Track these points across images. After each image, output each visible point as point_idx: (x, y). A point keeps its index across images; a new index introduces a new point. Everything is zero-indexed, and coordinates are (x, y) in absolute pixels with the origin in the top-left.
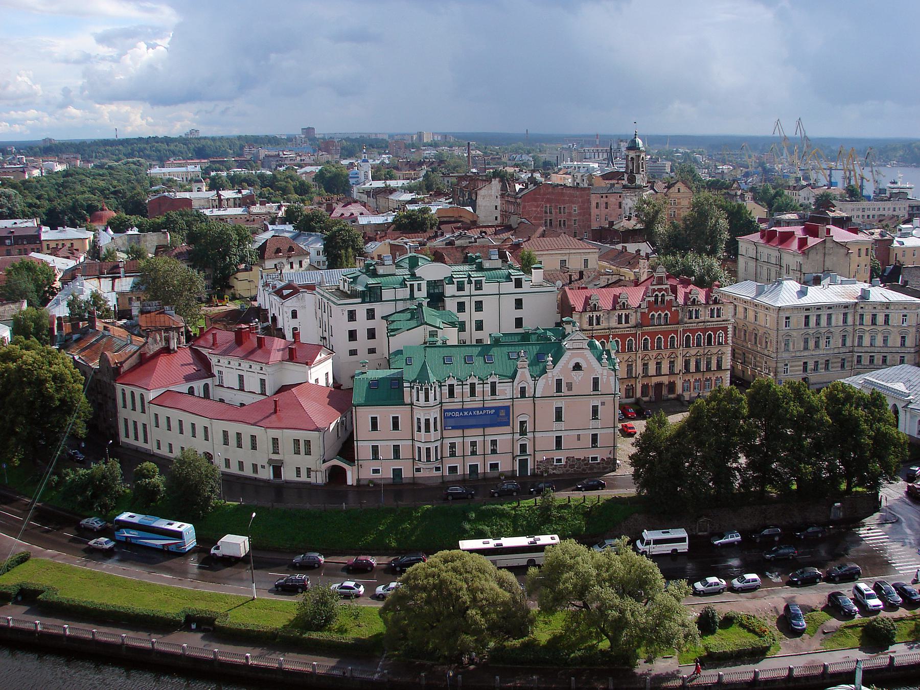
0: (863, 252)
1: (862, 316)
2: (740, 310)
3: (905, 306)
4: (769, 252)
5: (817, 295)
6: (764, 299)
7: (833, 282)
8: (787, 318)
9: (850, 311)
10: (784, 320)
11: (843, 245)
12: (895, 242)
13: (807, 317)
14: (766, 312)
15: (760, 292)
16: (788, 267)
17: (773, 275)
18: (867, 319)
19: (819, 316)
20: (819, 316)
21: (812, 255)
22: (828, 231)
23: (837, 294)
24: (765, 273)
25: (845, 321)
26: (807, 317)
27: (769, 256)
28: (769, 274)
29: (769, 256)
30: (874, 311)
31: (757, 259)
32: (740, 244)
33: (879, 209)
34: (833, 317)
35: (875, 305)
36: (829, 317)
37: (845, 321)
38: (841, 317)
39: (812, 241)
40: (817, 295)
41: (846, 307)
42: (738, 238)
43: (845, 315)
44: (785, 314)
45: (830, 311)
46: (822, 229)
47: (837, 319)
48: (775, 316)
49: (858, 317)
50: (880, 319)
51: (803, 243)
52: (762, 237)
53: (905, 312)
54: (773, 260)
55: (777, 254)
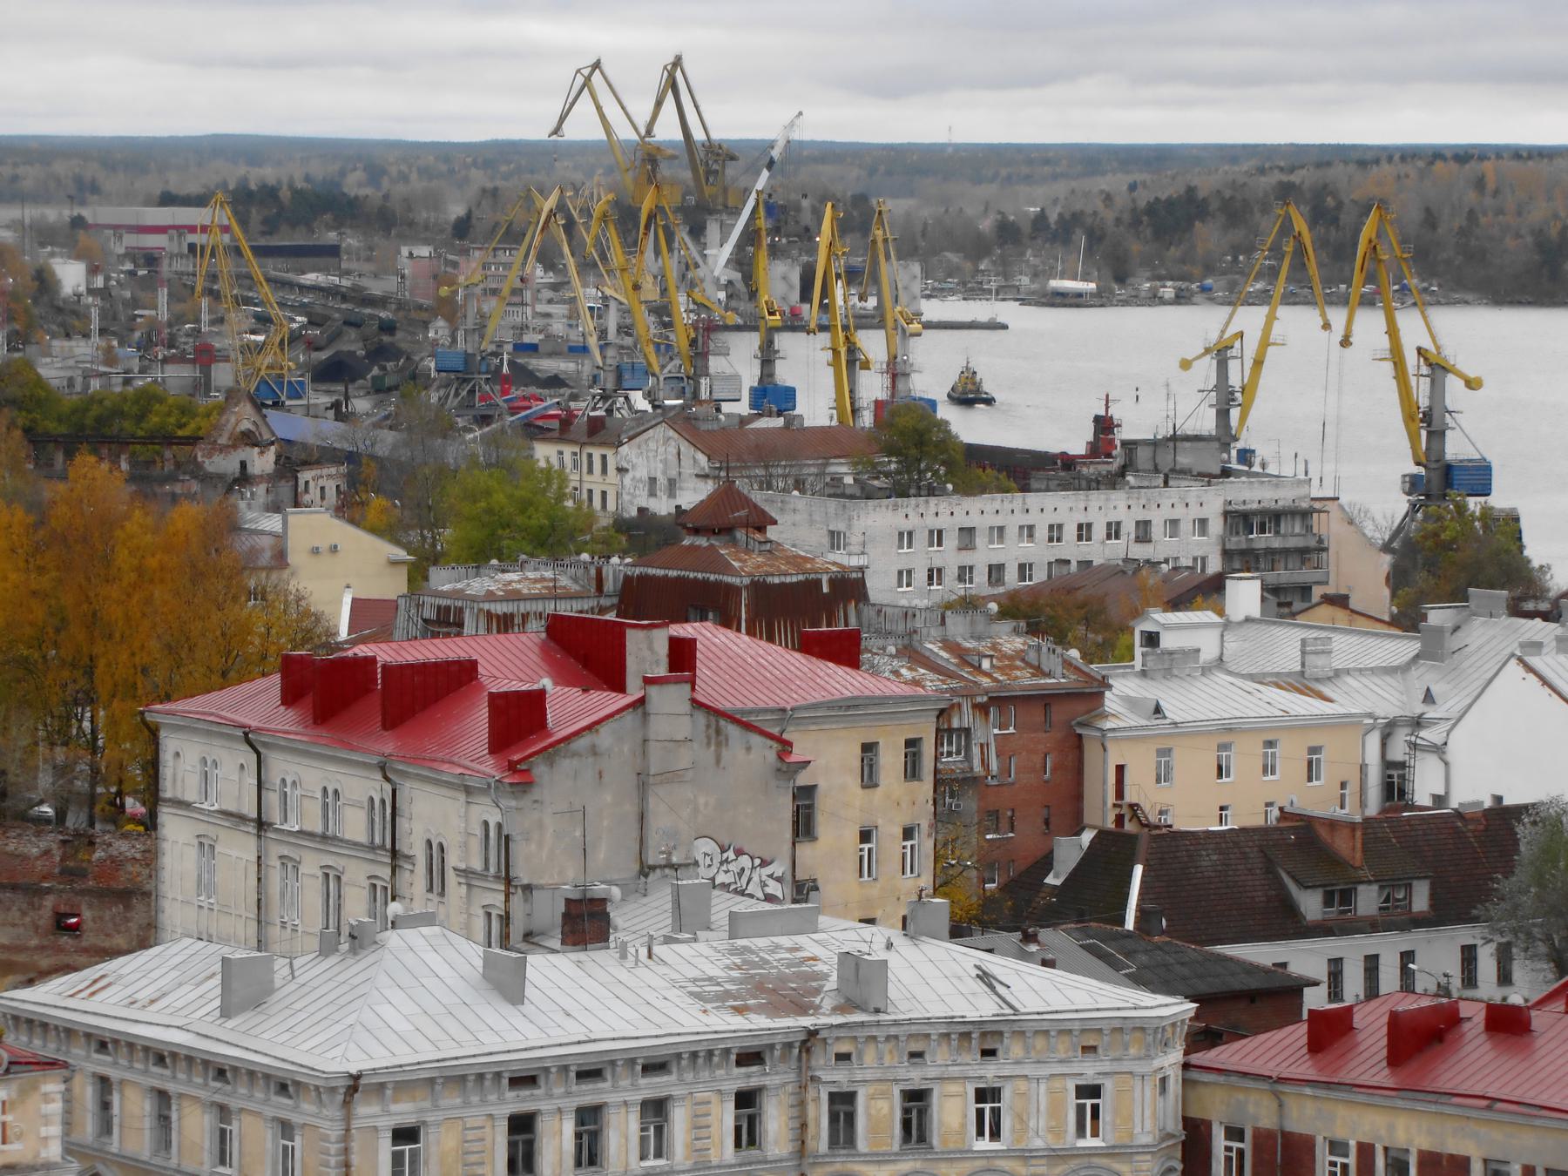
0: (891, 760)
1: (843, 1103)
2: (134, 1107)
3: (1088, 1037)
4: (329, 784)
5: (582, 1003)
6: (269, 1040)
7: (687, 920)
8: (405, 1134)
9: (774, 1079)
10: (386, 1148)
11: (773, 729)
12: (1111, 702)
13: (522, 1125)
14: (281, 1106)
15: (243, 991)
16: (436, 853)
17: (356, 908)
18: (878, 1113)
19: (590, 1120)
20: (590, 1120)
21: (558, 782)
22: (682, 656)
23: (706, 995)
24: (311, 894)
25: (748, 1135)
26: (522, 1125)
27: (331, 798)
28: (333, 903)
29: (331, 798)
30: (915, 1077)
31: (261, 825)
32: (170, 743)
33: (1055, 533)
34: (679, 1117)
35: (917, 1042)
36: (656, 1109)
37: (748, 1135)
38: (726, 1116)
39: (568, 706)
40: (582, 1003)
41: (750, 1058)
42: (158, 713)
43: (746, 1099)
44: (395, 1107)
45: (653, 1086)
46: (646, 650)
47: (699, 1126)
48: (335, 1132)
49: (820, 1115)
50: (952, 1112)
51: (518, 721)
52: (290, 697)
53: (1089, 1071)
54: (354, 825)
55: (375, 787)
